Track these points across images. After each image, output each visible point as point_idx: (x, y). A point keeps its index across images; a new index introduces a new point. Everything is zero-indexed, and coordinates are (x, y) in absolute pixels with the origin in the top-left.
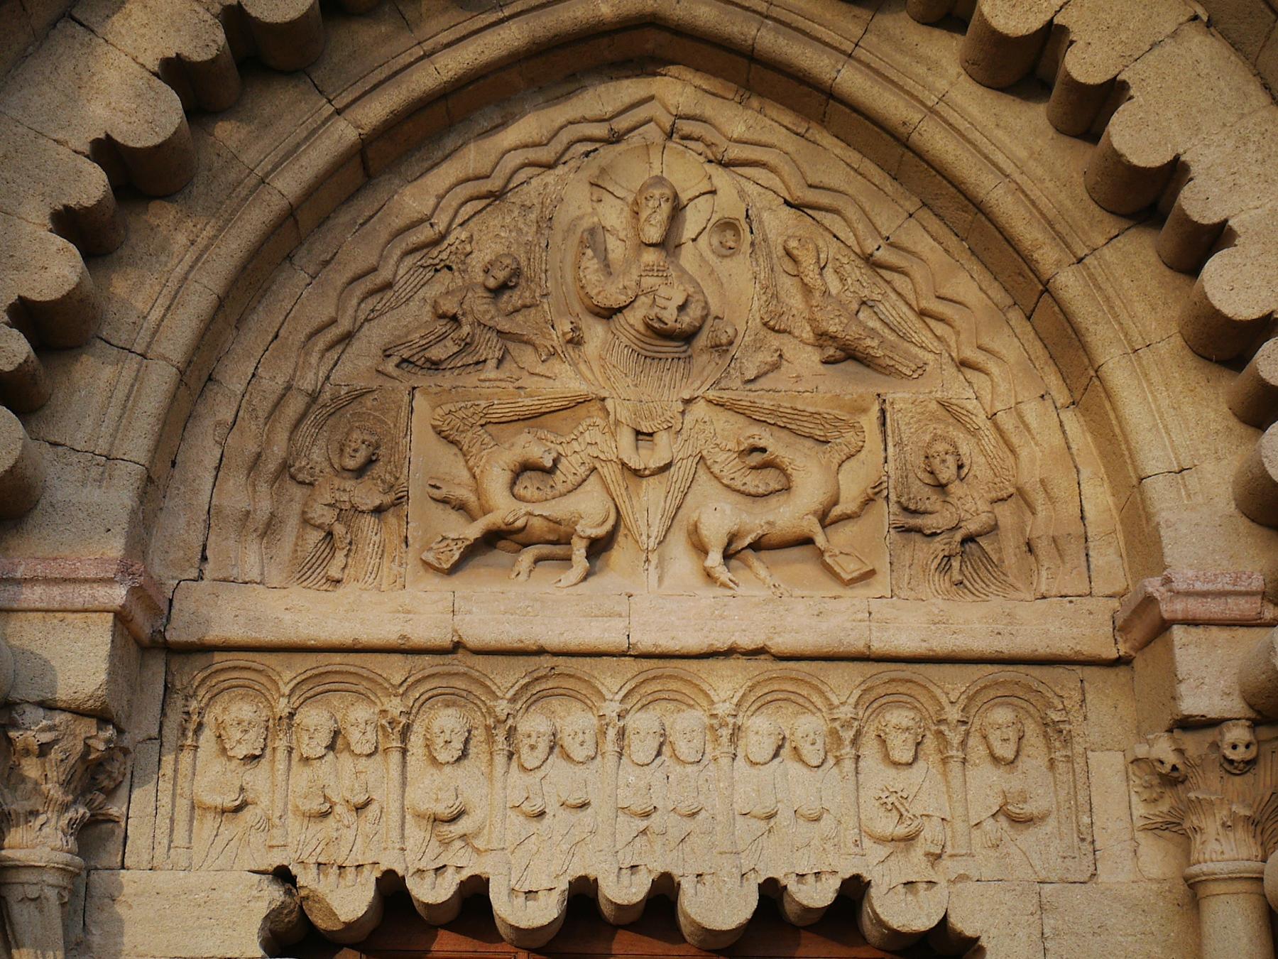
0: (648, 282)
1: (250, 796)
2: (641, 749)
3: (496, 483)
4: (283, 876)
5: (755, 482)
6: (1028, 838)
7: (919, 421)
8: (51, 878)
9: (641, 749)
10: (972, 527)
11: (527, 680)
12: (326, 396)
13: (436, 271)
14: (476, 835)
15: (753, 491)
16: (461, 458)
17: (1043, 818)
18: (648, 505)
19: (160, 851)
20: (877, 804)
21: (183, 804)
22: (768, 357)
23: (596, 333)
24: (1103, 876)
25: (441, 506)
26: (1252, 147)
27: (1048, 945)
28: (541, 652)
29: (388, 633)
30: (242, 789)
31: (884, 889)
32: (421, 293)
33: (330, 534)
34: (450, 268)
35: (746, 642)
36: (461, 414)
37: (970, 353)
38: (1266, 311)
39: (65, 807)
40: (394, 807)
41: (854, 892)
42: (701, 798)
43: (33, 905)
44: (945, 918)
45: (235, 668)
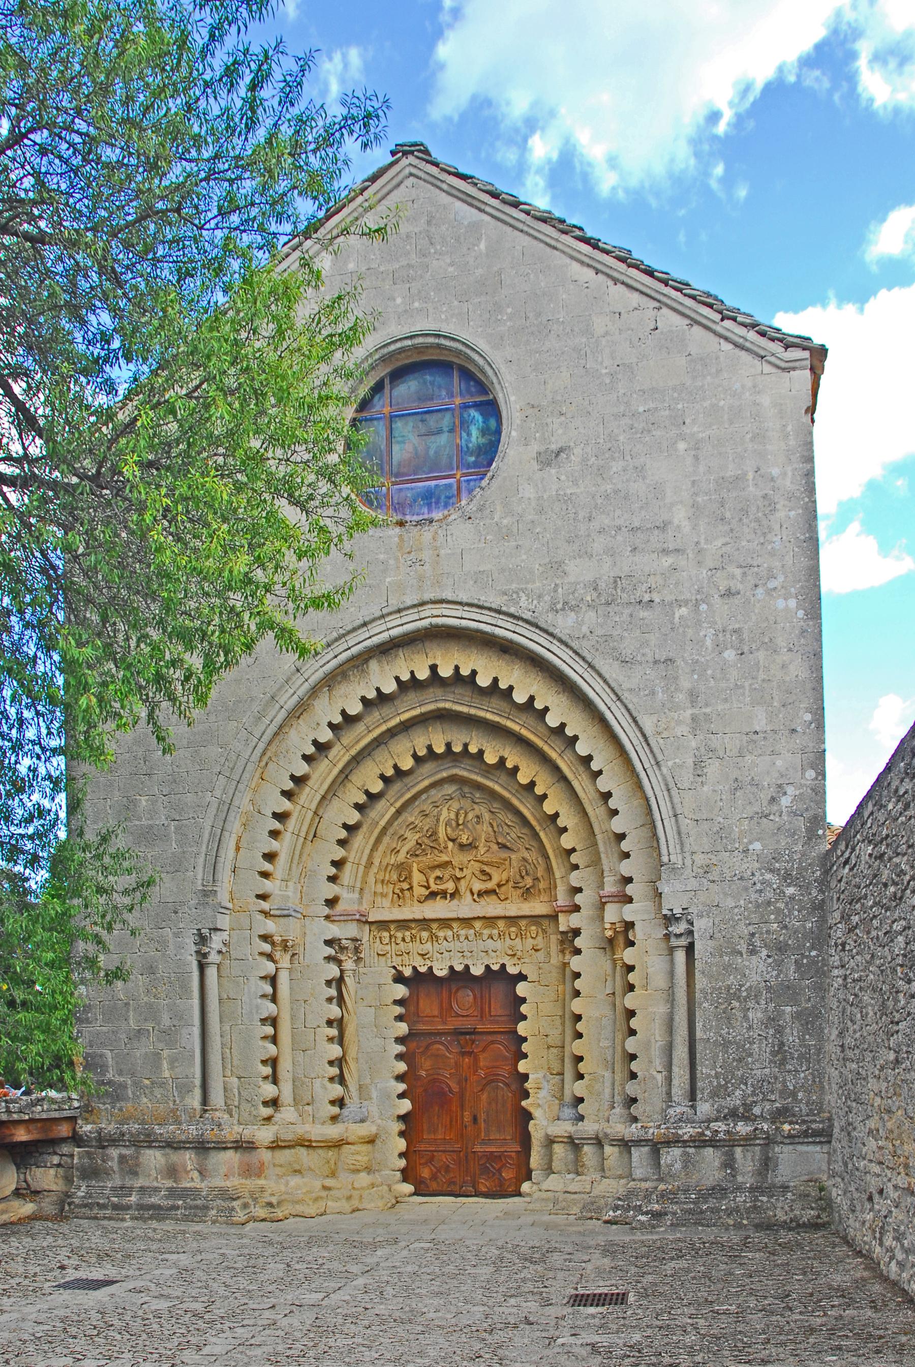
3: (432, 881)
4: (394, 967)
29: (410, 917)
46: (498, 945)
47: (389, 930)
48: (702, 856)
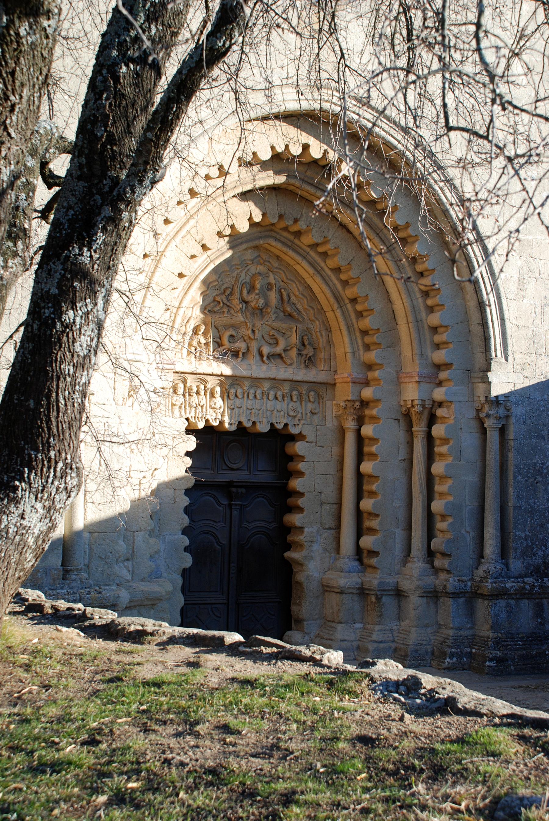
2: (251, 397)
4: (187, 419)
5: (271, 341)
6: (315, 417)
18: (254, 346)
35: (272, 377)
46: (279, 405)
48: (520, 356)
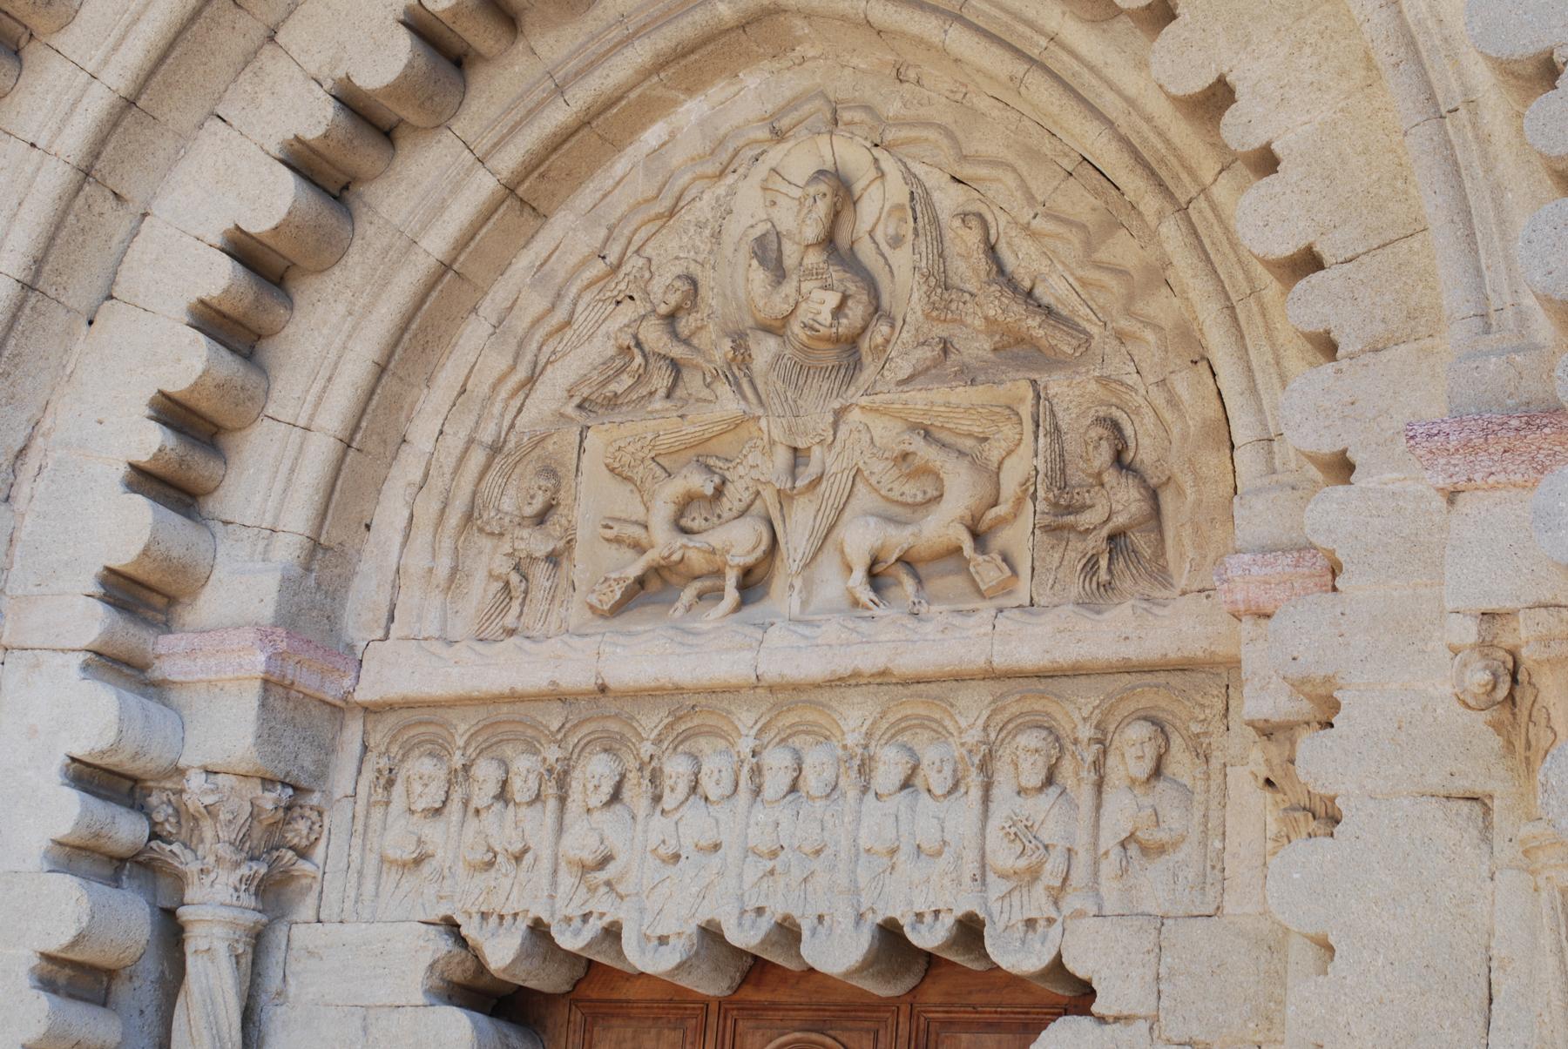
0: (807, 286)
1: (430, 849)
2: (776, 783)
5: (912, 491)
7: (1080, 404)
8: (218, 931)
9: (776, 783)
10: (1120, 520)
11: (670, 719)
12: (511, 444)
13: (618, 303)
14: (621, 879)
15: (910, 500)
16: (637, 495)
17: (1175, 845)
19: (348, 905)
20: (1001, 834)
21: (372, 859)
22: (927, 354)
23: (764, 350)
24: (1228, 909)
25: (615, 546)
26: (1308, 50)
27: (1162, 987)
28: (679, 689)
30: (420, 842)
31: (1001, 926)
32: (604, 328)
33: (507, 583)
34: (631, 298)
36: (631, 449)
37: (1124, 324)
38: (1302, 244)
39: (237, 865)
40: (546, 854)
41: (970, 931)
42: (826, 834)
43: (206, 956)
44: (1059, 956)
45: (420, 723)
47: (439, 751)
